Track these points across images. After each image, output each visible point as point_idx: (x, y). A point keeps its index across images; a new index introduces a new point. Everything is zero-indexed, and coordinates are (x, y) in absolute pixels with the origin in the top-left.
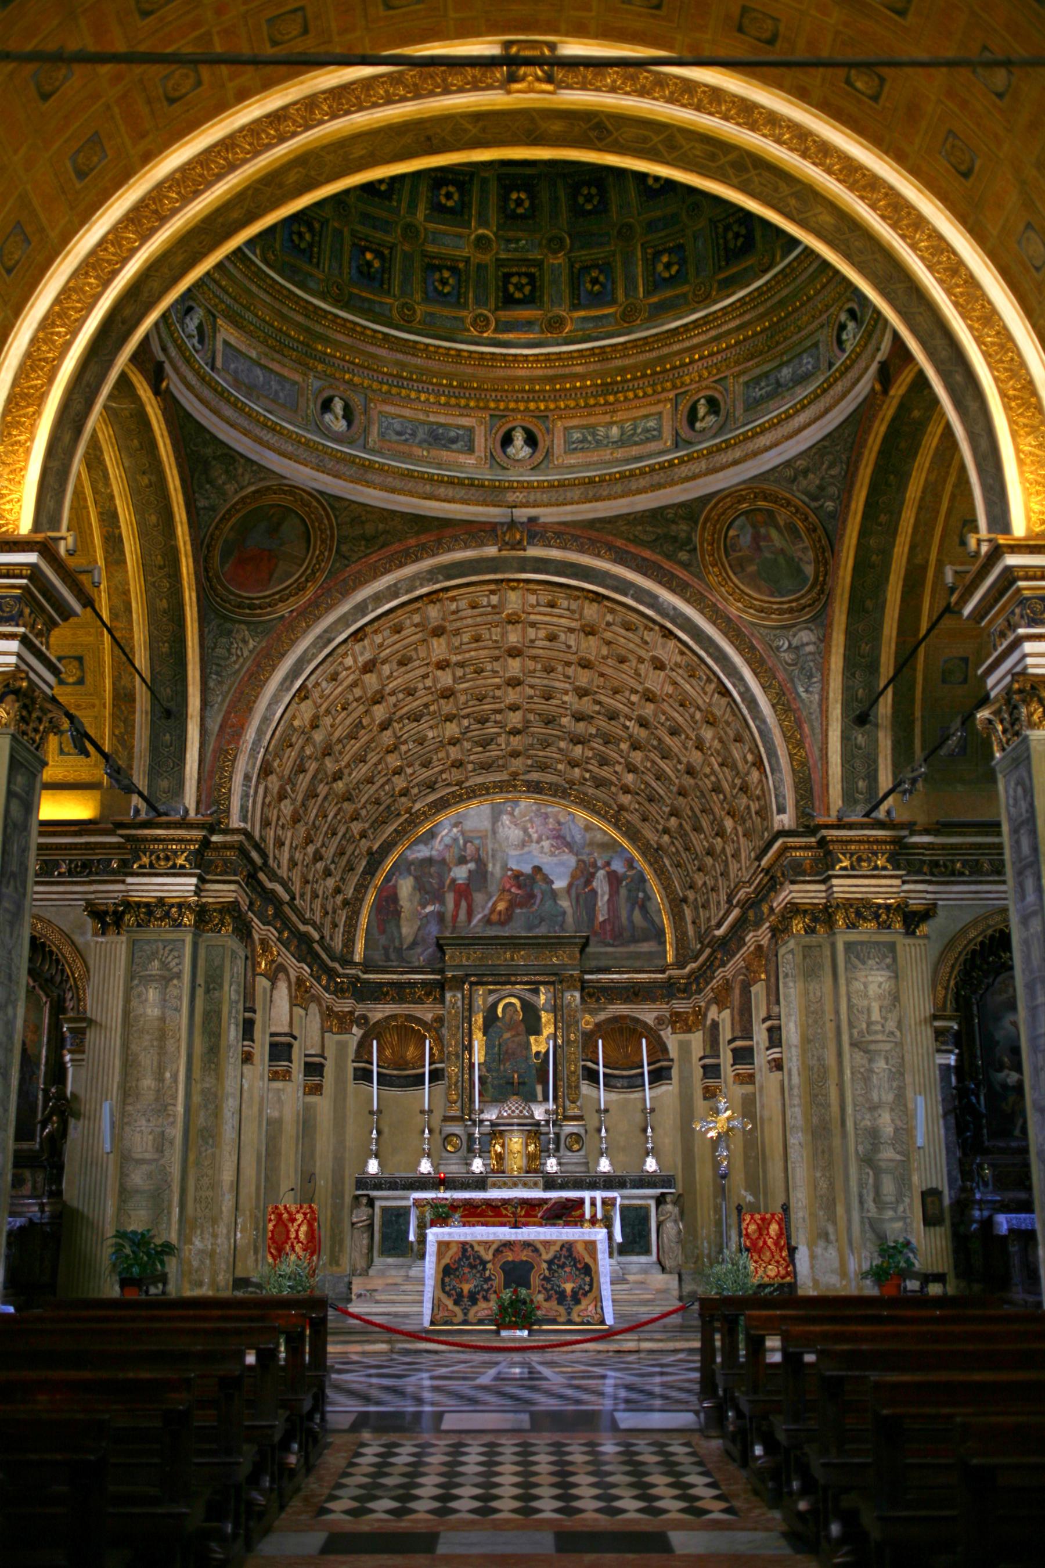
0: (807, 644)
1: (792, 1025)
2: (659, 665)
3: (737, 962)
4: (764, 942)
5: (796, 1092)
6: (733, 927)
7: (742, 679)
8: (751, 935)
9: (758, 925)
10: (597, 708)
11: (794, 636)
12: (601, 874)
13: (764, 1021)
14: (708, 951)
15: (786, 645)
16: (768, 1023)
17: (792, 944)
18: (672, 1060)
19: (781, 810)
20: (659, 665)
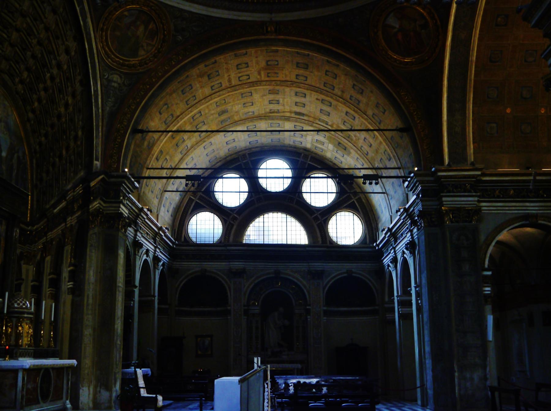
0: (115, 82)
1: (91, 273)
2: (67, 52)
3: (58, 230)
4: (73, 223)
5: (90, 307)
6: (61, 211)
7: (97, 83)
8: (70, 218)
9: (73, 213)
10: (40, 56)
11: (112, 74)
12: (16, 155)
13: (69, 267)
14: (45, 220)
15: (107, 76)
16: (71, 268)
17: (96, 230)
18: (23, 280)
19: (97, 160)
20: (67, 52)
